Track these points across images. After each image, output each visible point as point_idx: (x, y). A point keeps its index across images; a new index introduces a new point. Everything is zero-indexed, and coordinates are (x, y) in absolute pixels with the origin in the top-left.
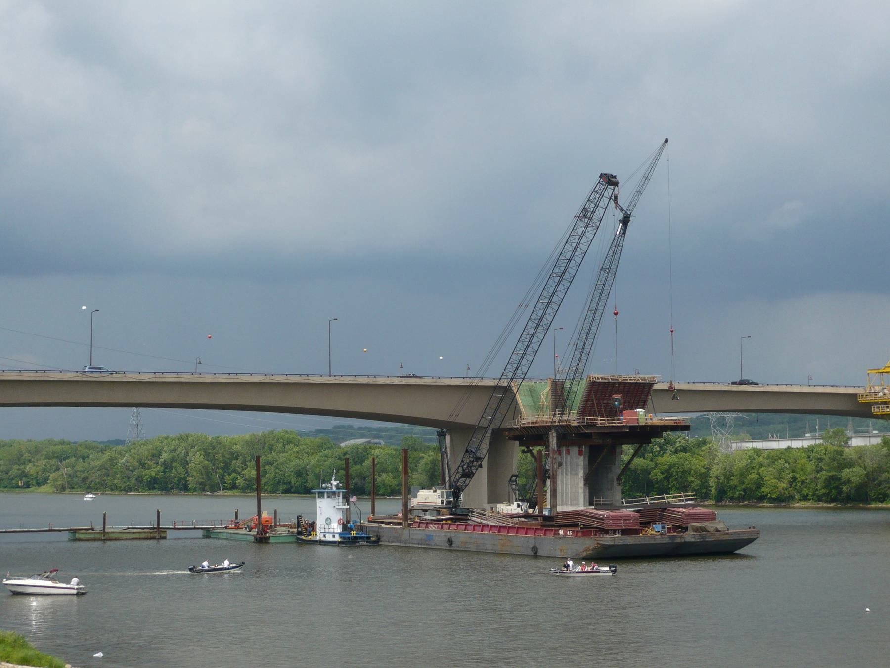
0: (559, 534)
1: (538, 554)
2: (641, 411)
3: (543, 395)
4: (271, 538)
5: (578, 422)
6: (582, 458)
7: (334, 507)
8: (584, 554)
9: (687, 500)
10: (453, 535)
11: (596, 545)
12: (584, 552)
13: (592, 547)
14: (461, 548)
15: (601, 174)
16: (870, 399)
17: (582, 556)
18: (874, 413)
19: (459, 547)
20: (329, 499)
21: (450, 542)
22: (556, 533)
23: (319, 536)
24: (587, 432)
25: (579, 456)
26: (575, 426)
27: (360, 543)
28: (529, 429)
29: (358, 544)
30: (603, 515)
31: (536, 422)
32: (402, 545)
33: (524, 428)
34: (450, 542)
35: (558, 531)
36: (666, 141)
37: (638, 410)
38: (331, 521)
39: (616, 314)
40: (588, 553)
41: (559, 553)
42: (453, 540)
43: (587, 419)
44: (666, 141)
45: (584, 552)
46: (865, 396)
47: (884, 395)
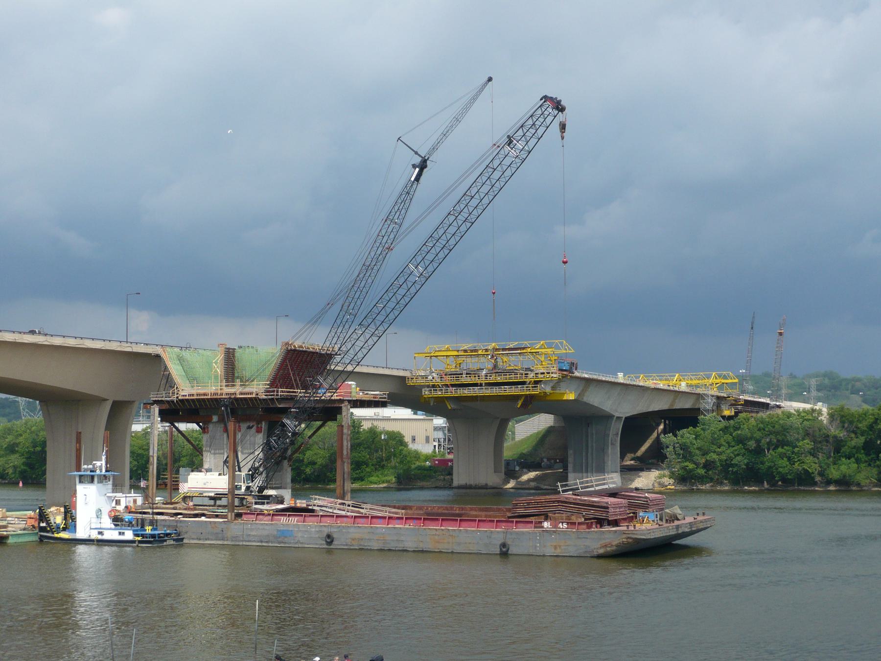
0: (543, 527)
1: (510, 552)
2: (353, 384)
3: (216, 363)
4: (10, 538)
5: (266, 395)
6: (260, 436)
7: (106, 494)
8: (601, 551)
9: (597, 485)
10: (333, 530)
11: (625, 540)
12: (601, 548)
13: (614, 543)
14: (353, 545)
15: (546, 95)
16: (421, 382)
17: (595, 553)
18: (424, 396)
19: (347, 545)
20: (99, 484)
21: (330, 539)
22: (539, 525)
23: (81, 532)
24: (280, 406)
25: (257, 434)
26: (264, 400)
27: (168, 541)
28: (213, 402)
29: (165, 543)
30: (607, 503)
31: (205, 394)
32: (226, 543)
33: (182, 401)
34: (330, 539)
35: (541, 522)
36: (490, 79)
37: (350, 383)
38: (101, 514)
39: (565, 263)
40: (609, 549)
41: (553, 550)
42: (335, 536)
43: (282, 392)
44: (490, 79)
45: (601, 548)
46: (410, 380)
47: (433, 378)
